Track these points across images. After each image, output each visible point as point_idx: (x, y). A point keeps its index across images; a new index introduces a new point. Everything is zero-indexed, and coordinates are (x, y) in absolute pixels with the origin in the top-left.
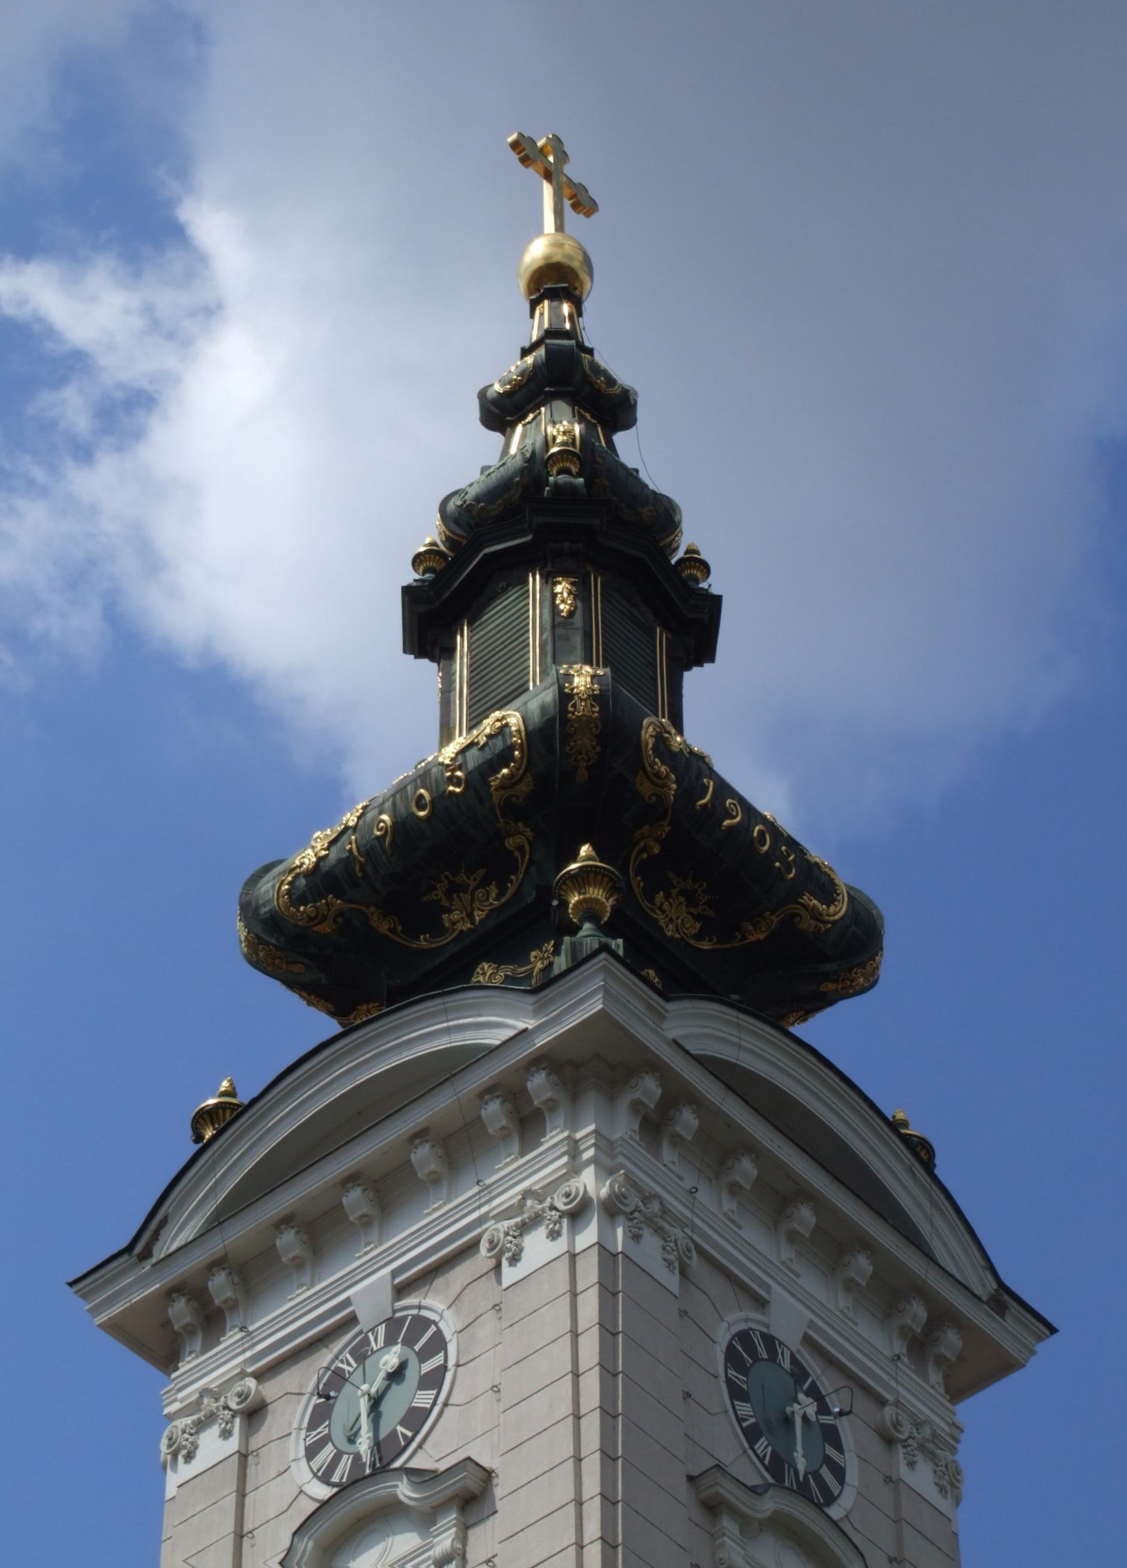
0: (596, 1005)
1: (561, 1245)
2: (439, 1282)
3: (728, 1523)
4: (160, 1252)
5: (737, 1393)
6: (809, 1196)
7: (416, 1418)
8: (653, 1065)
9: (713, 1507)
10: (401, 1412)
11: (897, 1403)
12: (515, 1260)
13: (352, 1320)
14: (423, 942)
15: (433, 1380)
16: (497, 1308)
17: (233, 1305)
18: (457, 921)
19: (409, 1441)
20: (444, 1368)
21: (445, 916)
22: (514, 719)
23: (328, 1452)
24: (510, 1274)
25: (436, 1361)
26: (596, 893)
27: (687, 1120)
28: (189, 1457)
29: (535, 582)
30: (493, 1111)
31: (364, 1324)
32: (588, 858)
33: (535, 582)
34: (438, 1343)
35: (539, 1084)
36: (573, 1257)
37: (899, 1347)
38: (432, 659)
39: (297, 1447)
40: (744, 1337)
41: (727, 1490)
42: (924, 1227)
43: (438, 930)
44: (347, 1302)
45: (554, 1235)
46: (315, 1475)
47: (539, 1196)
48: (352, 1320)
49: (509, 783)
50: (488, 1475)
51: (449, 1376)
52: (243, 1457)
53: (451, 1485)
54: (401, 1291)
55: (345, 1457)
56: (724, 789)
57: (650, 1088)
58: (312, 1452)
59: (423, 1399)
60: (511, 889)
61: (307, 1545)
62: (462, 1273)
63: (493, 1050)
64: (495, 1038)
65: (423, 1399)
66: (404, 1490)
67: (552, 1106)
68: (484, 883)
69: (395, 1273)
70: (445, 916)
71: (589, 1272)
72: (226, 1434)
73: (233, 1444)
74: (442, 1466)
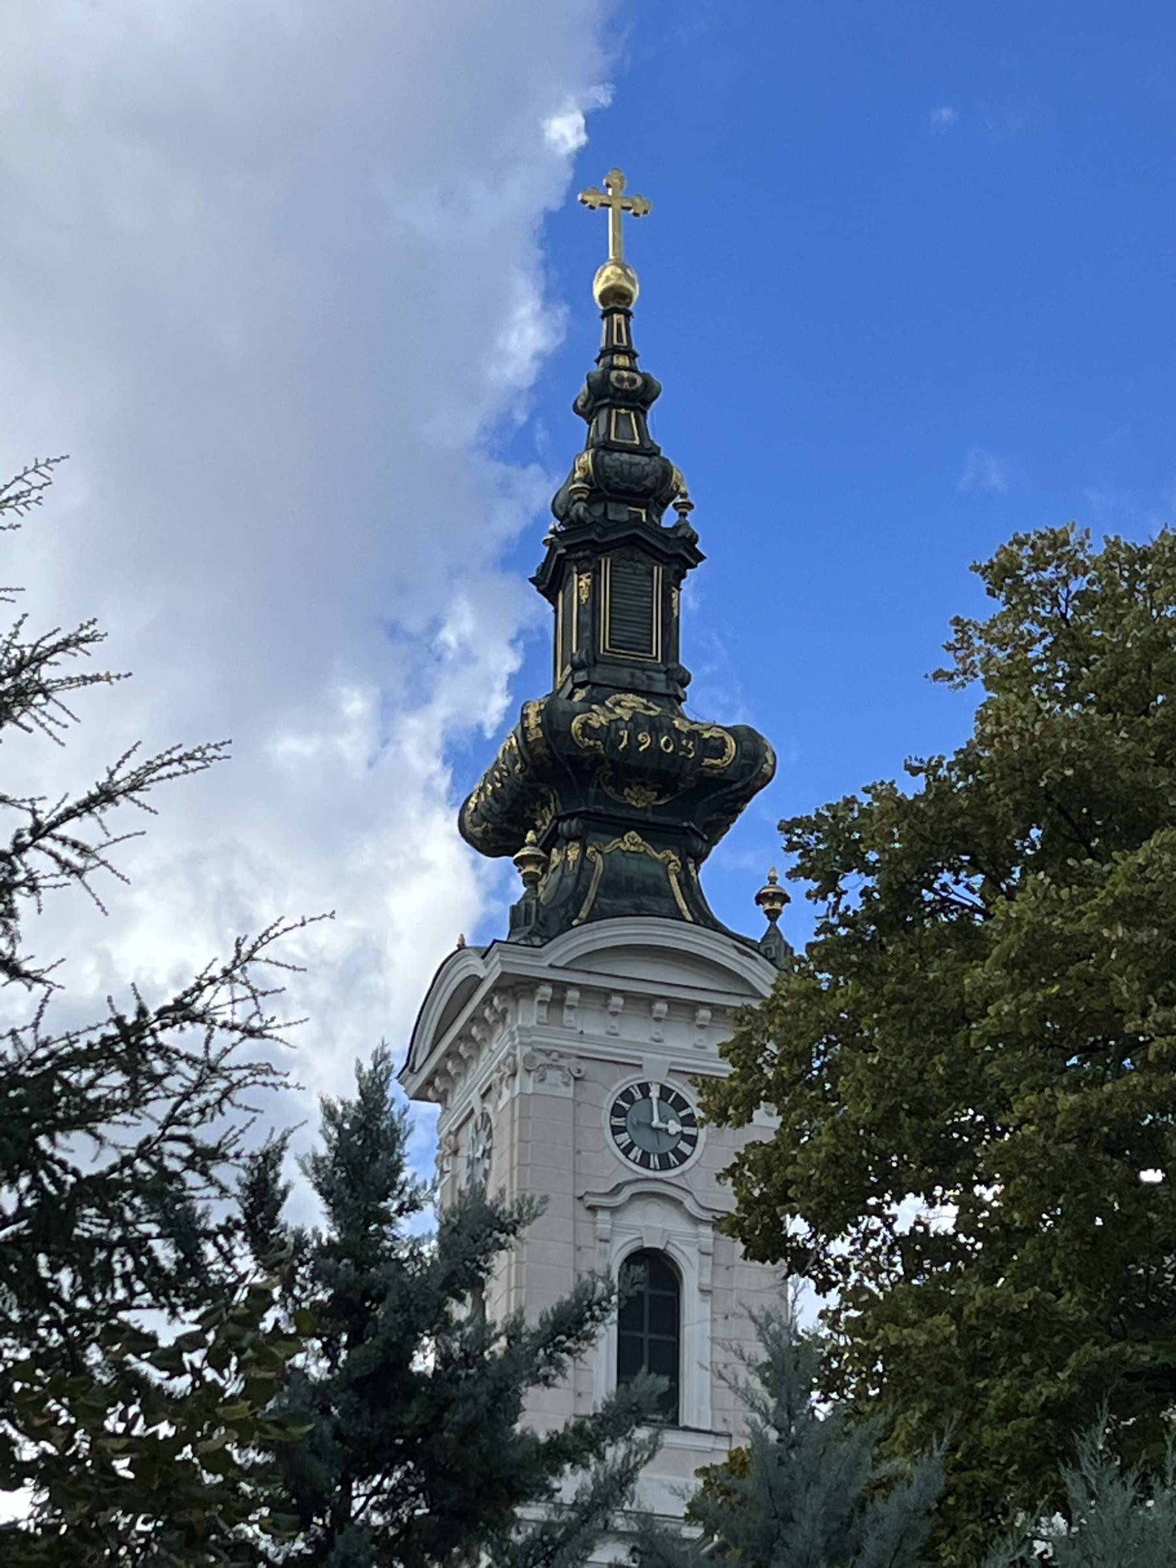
7: (683, 1158)
10: (672, 1147)
13: (640, 1066)
19: (676, 1166)
21: (627, 790)
23: (624, 1138)
39: (605, 1119)
44: (640, 1058)
46: (619, 1145)
55: (636, 1148)
58: (616, 1130)
59: (684, 1147)
60: (662, 802)
65: (684, 1147)
66: (688, 1203)
69: (673, 1063)
70: (627, 790)
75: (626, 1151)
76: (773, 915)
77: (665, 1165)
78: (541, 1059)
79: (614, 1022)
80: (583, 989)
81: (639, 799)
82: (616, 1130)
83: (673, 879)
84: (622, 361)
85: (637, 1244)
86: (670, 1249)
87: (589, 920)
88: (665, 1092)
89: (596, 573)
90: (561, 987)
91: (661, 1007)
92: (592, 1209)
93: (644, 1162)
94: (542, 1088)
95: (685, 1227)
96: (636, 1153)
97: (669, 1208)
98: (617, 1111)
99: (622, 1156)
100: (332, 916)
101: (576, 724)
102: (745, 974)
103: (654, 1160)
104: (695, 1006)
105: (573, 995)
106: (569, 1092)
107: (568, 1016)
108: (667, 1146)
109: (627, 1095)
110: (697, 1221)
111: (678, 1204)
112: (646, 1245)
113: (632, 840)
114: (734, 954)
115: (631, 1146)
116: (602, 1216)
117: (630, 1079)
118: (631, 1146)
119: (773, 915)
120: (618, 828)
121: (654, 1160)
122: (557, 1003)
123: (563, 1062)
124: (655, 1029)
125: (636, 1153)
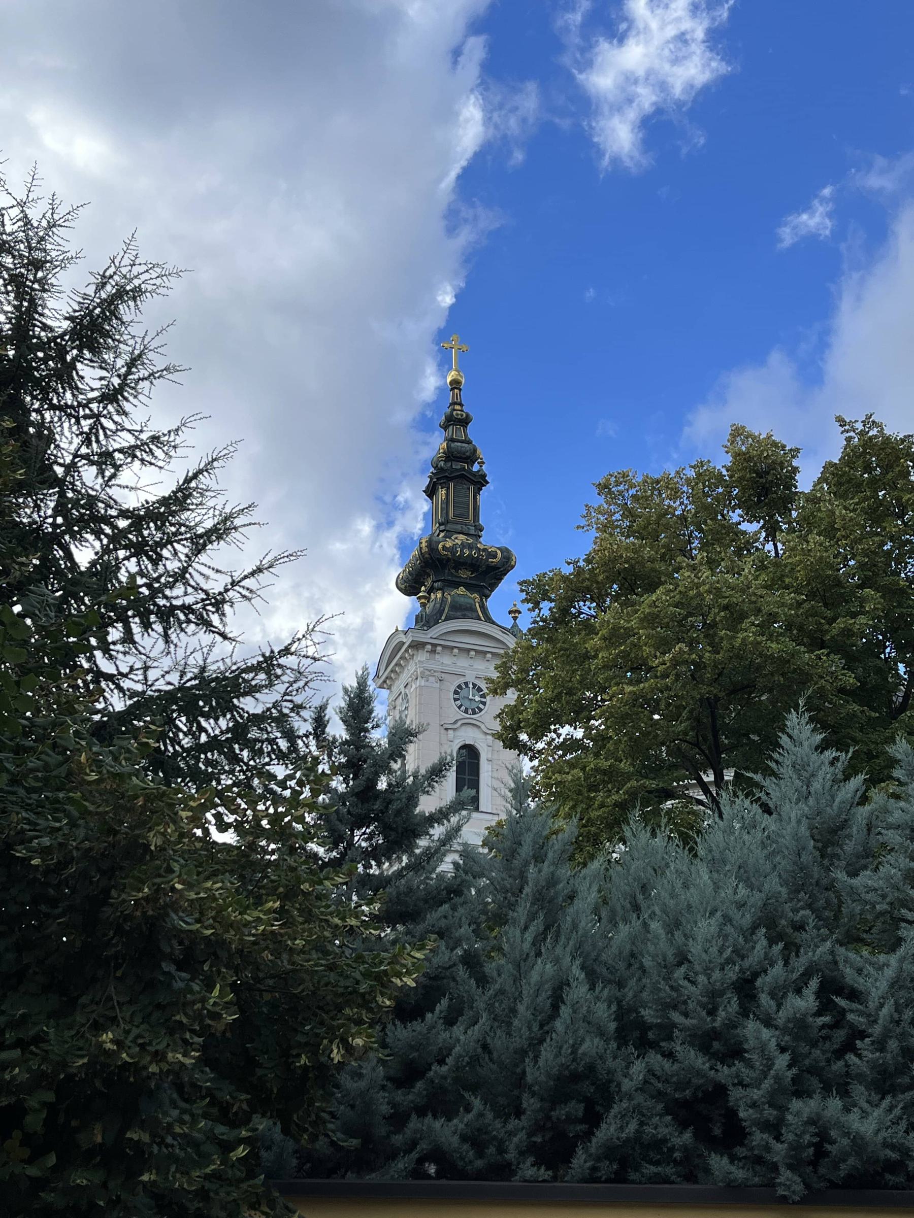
7: (481, 710)
23: (459, 703)
39: (451, 695)
58: (455, 700)
59: (481, 706)
65: (481, 706)
66: (483, 727)
75: (459, 707)
76: (515, 618)
77: (474, 713)
78: (427, 673)
79: (455, 659)
80: (444, 647)
81: (464, 574)
82: (455, 700)
83: (477, 605)
84: (458, 407)
87: (446, 620)
89: (448, 488)
90: (434, 645)
91: (473, 653)
92: (446, 729)
93: (466, 712)
94: (427, 684)
95: (482, 736)
96: (463, 708)
97: (475, 729)
98: (456, 692)
100: (343, 613)
101: (440, 546)
102: (505, 641)
103: (470, 711)
104: (486, 653)
105: (439, 649)
106: (438, 685)
107: (437, 656)
108: (474, 706)
109: (459, 687)
110: (486, 734)
111: (478, 727)
113: (461, 590)
114: (501, 633)
115: (461, 705)
116: (450, 732)
117: (461, 680)
118: (461, 705)
119: (515, 618)
120: (456, 585)
121: (470, 711)
122: (433, 652)
123: (436, 674)
124: (471, 662)
125: (463, 708)
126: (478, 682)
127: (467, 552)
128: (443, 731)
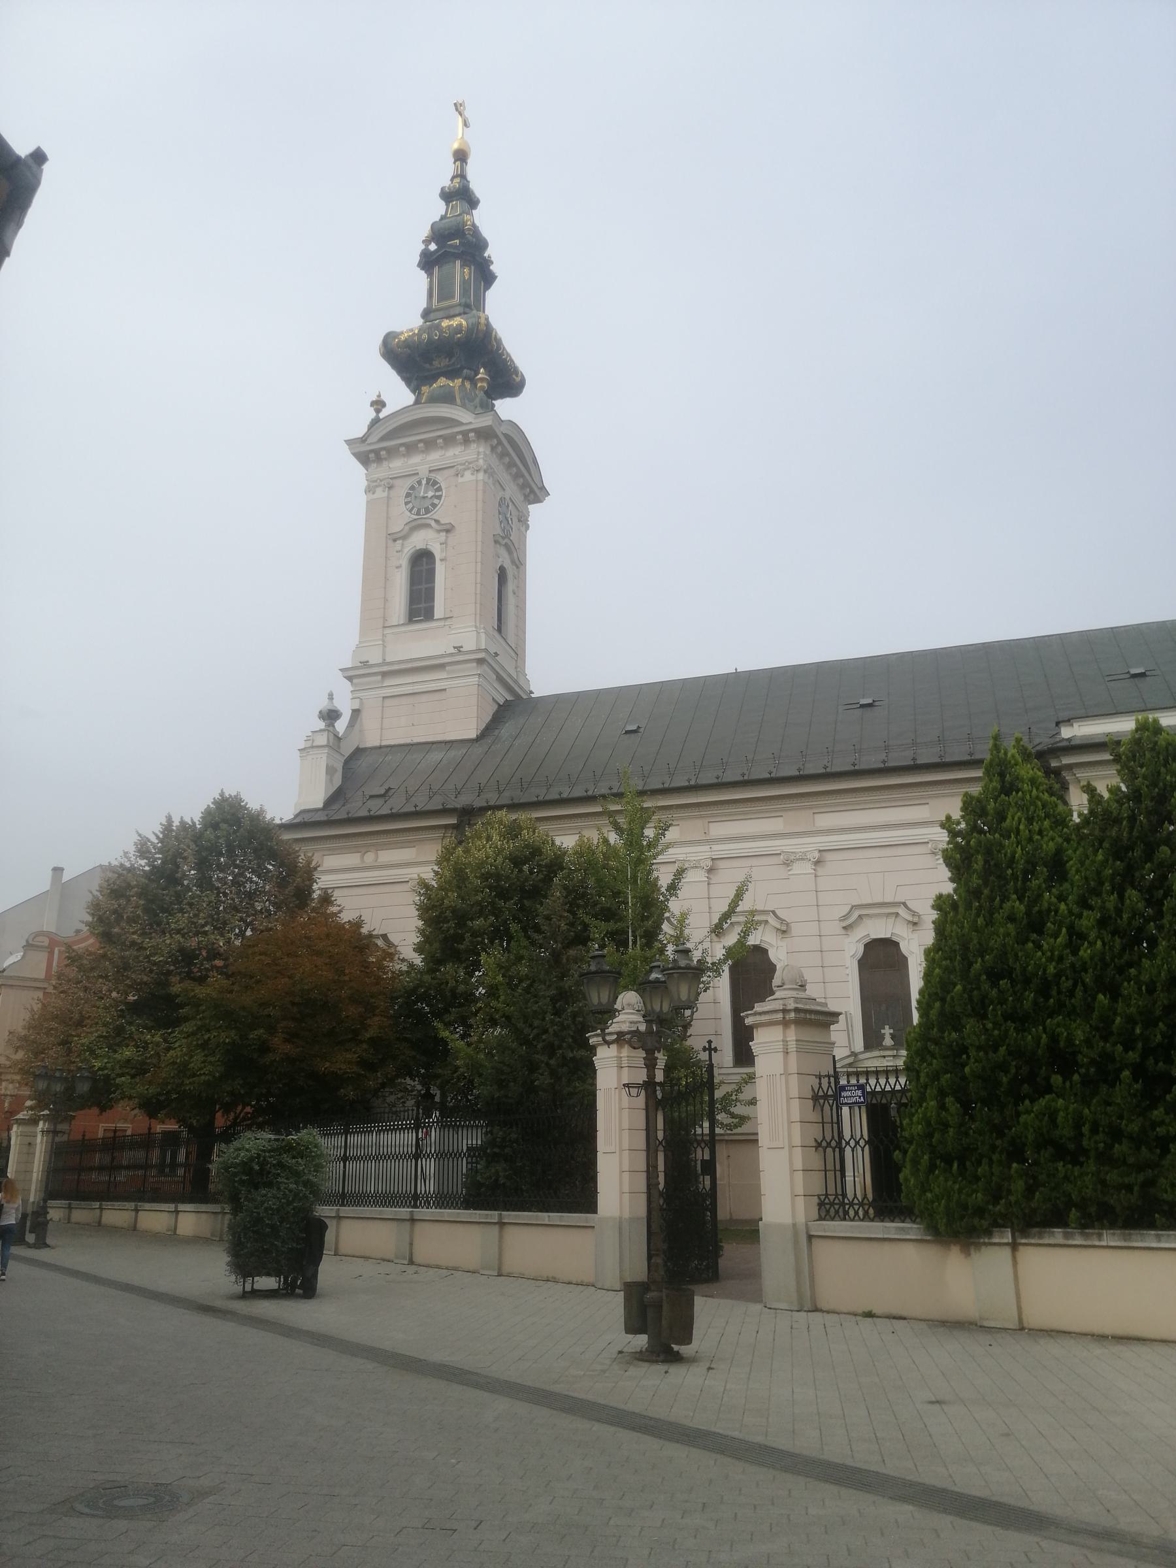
0: (489, 423)
1: (474, 478)
2: (441, 472)
3: (498, 546)
4: (369, 441)
5: (500, 513)
6: (515, 465)
7: (434, 506)
8: (496, 436)
9: (496, 542)
11: (522, 512)
12: (462, 476)
13: (418, 473)
14: (427, 366)
15: (439, 497)
16: (456, 486)
17: (386, 459)
18: (436, 363)
20: (441, 496)
22: (464, 323)
23: (410, 505)
24: (460, 480)
25: (440, 493)
26: (485, 385)
27: (500, 449)
28: (373, 493)
29: (458, 263)
30: (460, 437)
31: (421, 475)
32: (482, 373)
33: (458, 263)
34: (440, 489)
35: (472, 435)
36: (477, 481)
37: (522, 498)
38: (426, 272)
39: (402, 500)
40: (501, 499)
41: (500, 540)
42: (533, 473)
43: (431, 364)
44: (416, 470)
45: (472, 474)
47: (470, 463)
48: (418, 473)
49: (459, 338)
50: (453, 526)
51: (443, 498)
52: (388, 498)
53: (445, 527)
54: (430, 471)
56: (504, 348)
57: (495, 442)
58: (406, 503)
59: (436, 501)
60: (453, 361)
61: (407, 528)
62: (446, 472)
63: (462, 424)
64: (464, 421)
65: (436, 501)
67: (474, 441)
68: (445, 358)
69: (430, 467)
71: (480, 487)
72: (384, 491)
73: (385, 494)
74: (442, 522)
75: (410, 511)
77: (427, 511)
81: (440, 363)
82: (406, 503)
85: (414, 549)
86: (428, 547)
88: (428, 480)
90: (377, 452)
94: (375, 496)
96: (415, 510)
98: (408, 495)
99: (409, 514)
105: (383, 453)
107: (385, 464)
108: (427, 503)
109: (412, 488)
110: (439, 531)
111: (428, 526)
112: (418, 548)
126: (433, 475)
127: (425, 336)
128: (390, 542)
